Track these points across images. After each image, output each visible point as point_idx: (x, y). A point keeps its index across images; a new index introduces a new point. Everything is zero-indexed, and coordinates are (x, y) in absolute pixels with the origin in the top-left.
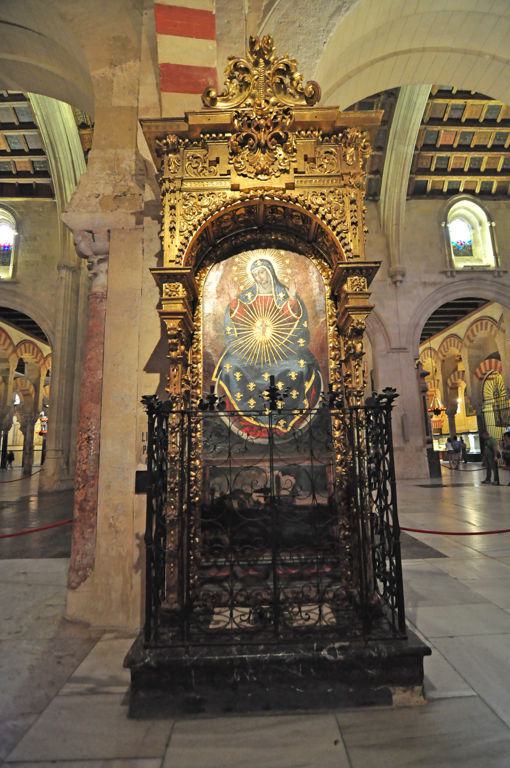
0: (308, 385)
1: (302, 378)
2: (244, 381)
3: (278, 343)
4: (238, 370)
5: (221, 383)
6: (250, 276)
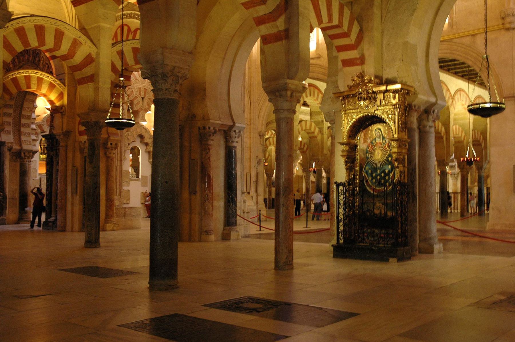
0: (391, 175)
1: (390, 172)
2: (372, 173)
4: (369, 169)
6: (374, 135)
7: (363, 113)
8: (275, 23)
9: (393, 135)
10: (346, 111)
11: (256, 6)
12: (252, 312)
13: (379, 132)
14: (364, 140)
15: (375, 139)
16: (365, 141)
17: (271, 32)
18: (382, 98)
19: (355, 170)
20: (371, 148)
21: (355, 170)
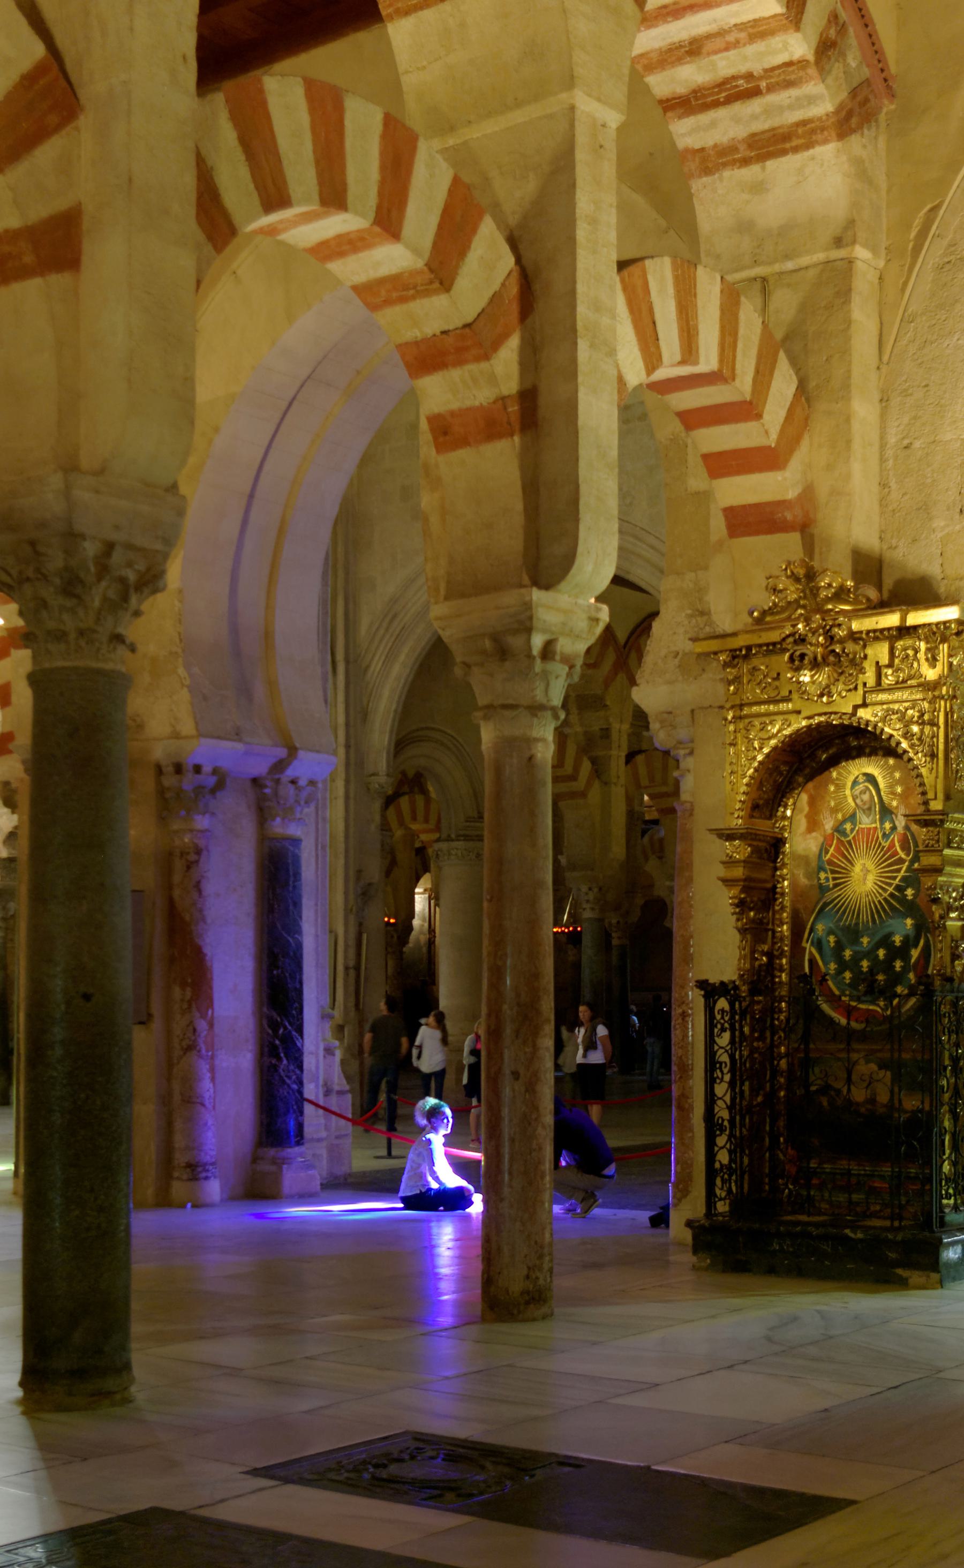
0: (915, 953)
1: (909, 943)
2: (839, 947)
3: (881, 895)
4: (830, 932)
5: (814, 951)
6: (850, 800)
7: (809, 718)
8: (484, 365)
9: (926, 803)
10: (741, 706)
11: (413, 298)
12: (441, 1496)
13: (868, 788)
14: (808, 822)
15: (852, 818)
16: (813, 824)
17: (468, 403)
18: (885, 660)
19: (773, 937)
20: (837, 849)
21: (773, 937)
